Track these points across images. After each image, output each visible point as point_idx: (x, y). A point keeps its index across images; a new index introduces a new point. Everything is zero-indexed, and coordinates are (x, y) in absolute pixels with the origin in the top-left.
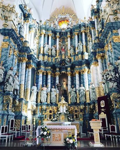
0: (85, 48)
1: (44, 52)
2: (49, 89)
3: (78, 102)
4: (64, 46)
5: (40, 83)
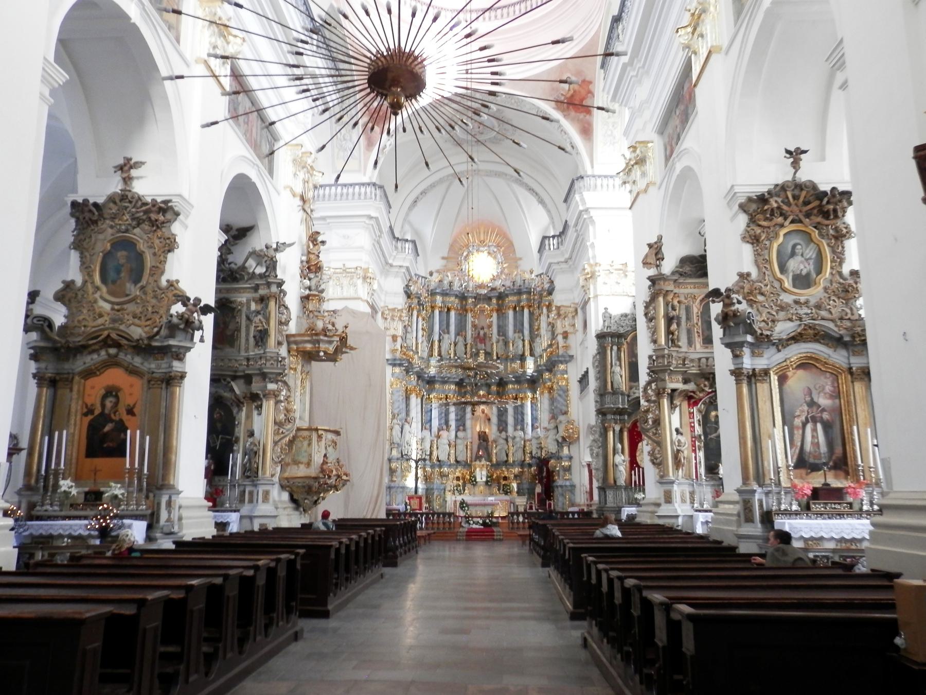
2: (453, 433)
3: (511, 460)
4: (483, 328)
5: (435, 423)
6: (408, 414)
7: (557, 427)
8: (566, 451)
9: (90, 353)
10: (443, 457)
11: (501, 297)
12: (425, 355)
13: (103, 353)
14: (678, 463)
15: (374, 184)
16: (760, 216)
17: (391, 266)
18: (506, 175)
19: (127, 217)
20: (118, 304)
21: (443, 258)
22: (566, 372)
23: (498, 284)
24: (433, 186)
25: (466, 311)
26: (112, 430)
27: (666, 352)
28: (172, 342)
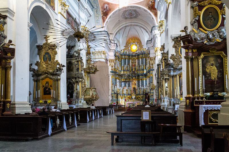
0: (144, 67)
1: (124, 69)
2: (127, 88)
3: (141, 93)
6: (116, 83)
7: (150, 86)
8: (152, 91)
9: (43, 75)
10: (125, 93)
11: (138, 55)
12: (120, 70)
13: (45, 75)
14: (166, 94)
15: (105, 31)
16: (177, 42)
17: (111, 49)
18: (138, 25)
19: (47, 48)
20: (47, 65)
21: (124, 46)
22: (152, 73)
23: (137, 52)
24: (121, 29)
25: (130, 59)
26: (48, 90)
27: (164, 70)
28: (57, 73)
